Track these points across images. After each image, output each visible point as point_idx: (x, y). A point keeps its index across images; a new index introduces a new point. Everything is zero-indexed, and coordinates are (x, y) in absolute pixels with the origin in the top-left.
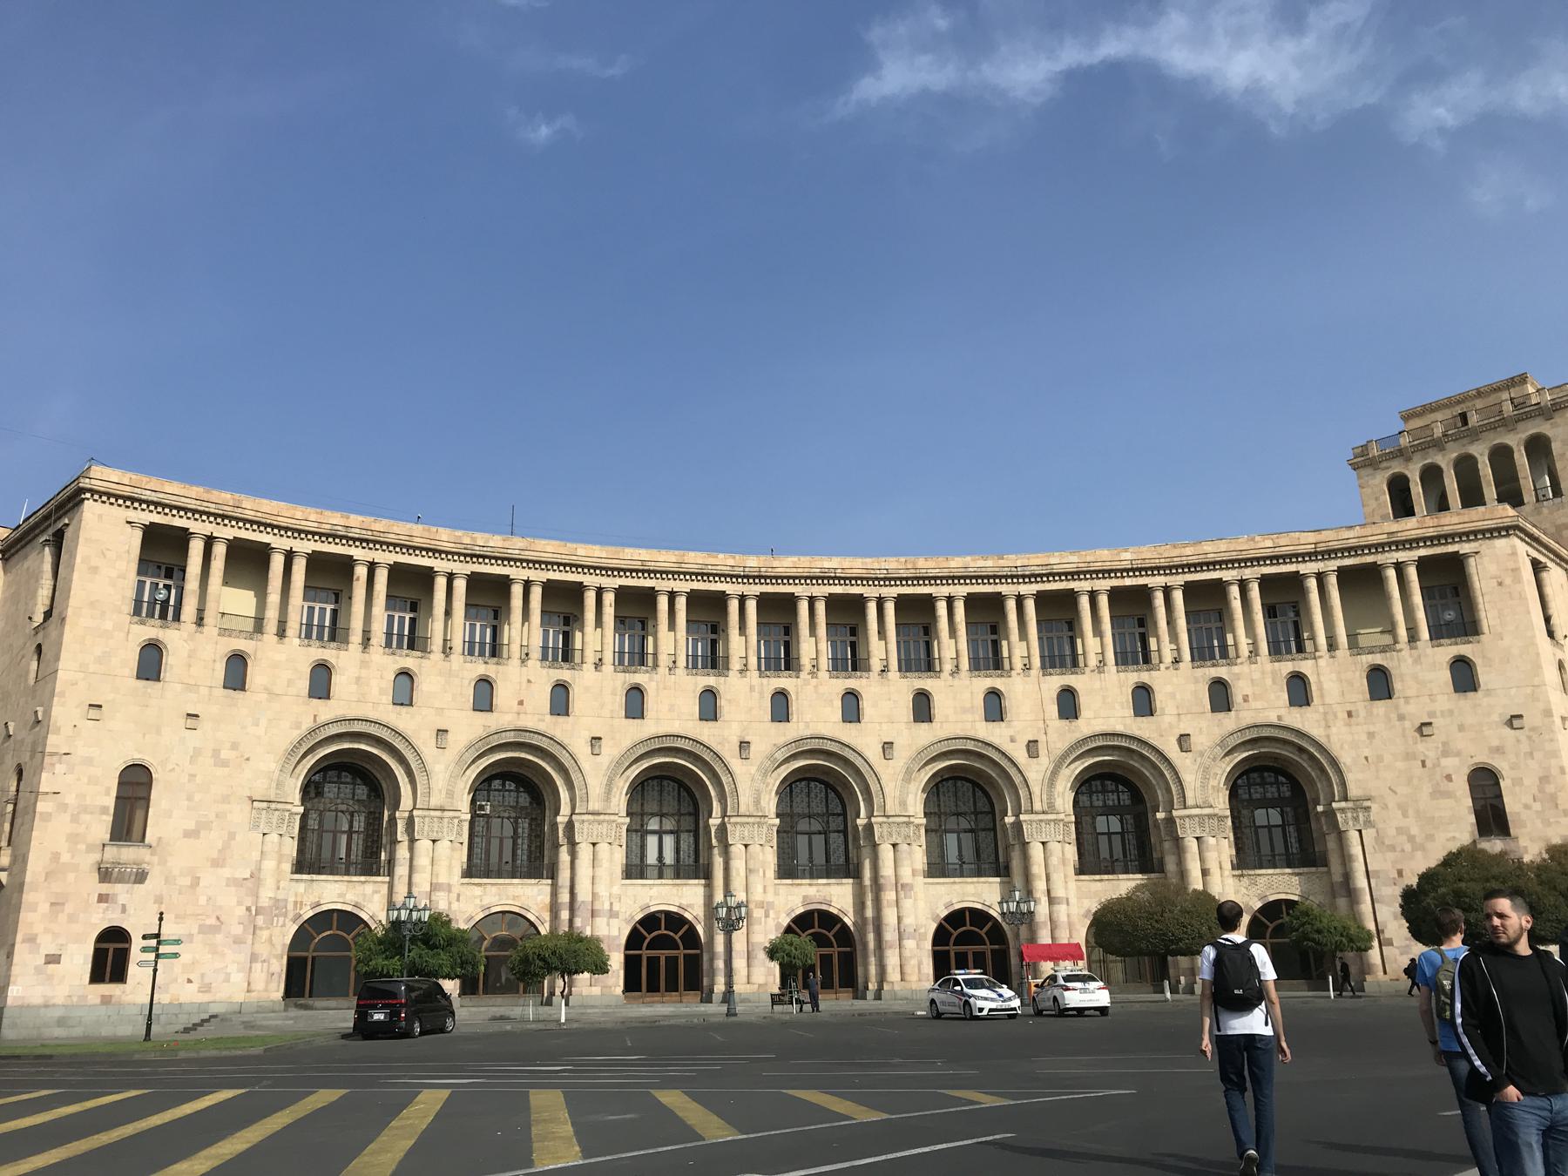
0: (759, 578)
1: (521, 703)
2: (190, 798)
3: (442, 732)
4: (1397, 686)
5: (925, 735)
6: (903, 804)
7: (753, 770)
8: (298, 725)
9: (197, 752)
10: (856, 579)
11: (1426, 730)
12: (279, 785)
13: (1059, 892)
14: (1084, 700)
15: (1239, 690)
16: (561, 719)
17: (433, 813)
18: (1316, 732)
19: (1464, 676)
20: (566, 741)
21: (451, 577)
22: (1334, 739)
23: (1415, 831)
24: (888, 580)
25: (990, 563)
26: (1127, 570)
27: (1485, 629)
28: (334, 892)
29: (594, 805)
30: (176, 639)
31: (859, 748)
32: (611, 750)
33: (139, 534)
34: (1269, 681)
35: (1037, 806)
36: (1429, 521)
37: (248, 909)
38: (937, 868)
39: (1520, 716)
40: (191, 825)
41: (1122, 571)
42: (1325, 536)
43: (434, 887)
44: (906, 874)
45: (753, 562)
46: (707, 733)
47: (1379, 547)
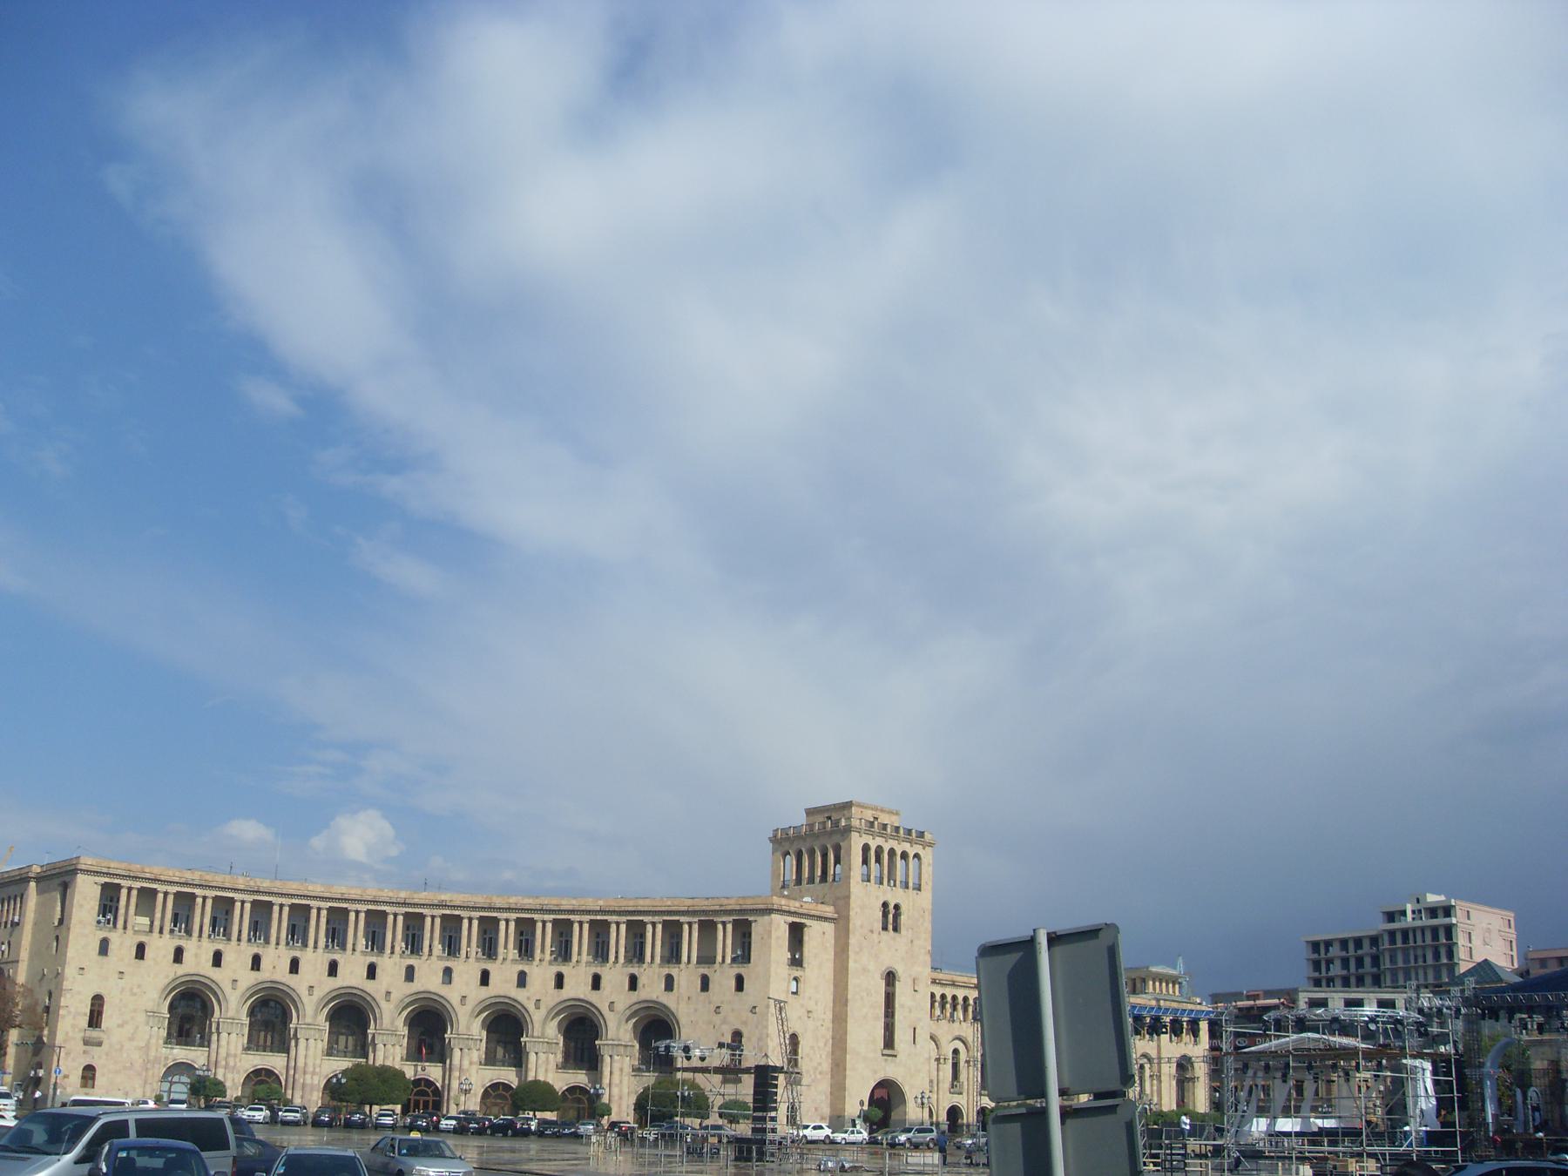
0: (405, 904)
5: (485, 993)
6: (468, 1028)
9: (123, 990)
14: (566, 980)
15: (641, 981)
18: (672, 1005)
19: (740, 983)
21: (243, 902)
24: (474, 908)
28: (181, 1053)
29: (308, 1020)
30: (115, 937)
32: (319, 993)
38: (490, 1060)
44: (466, 1063)
46: (369, 986)
47: (716, 913)
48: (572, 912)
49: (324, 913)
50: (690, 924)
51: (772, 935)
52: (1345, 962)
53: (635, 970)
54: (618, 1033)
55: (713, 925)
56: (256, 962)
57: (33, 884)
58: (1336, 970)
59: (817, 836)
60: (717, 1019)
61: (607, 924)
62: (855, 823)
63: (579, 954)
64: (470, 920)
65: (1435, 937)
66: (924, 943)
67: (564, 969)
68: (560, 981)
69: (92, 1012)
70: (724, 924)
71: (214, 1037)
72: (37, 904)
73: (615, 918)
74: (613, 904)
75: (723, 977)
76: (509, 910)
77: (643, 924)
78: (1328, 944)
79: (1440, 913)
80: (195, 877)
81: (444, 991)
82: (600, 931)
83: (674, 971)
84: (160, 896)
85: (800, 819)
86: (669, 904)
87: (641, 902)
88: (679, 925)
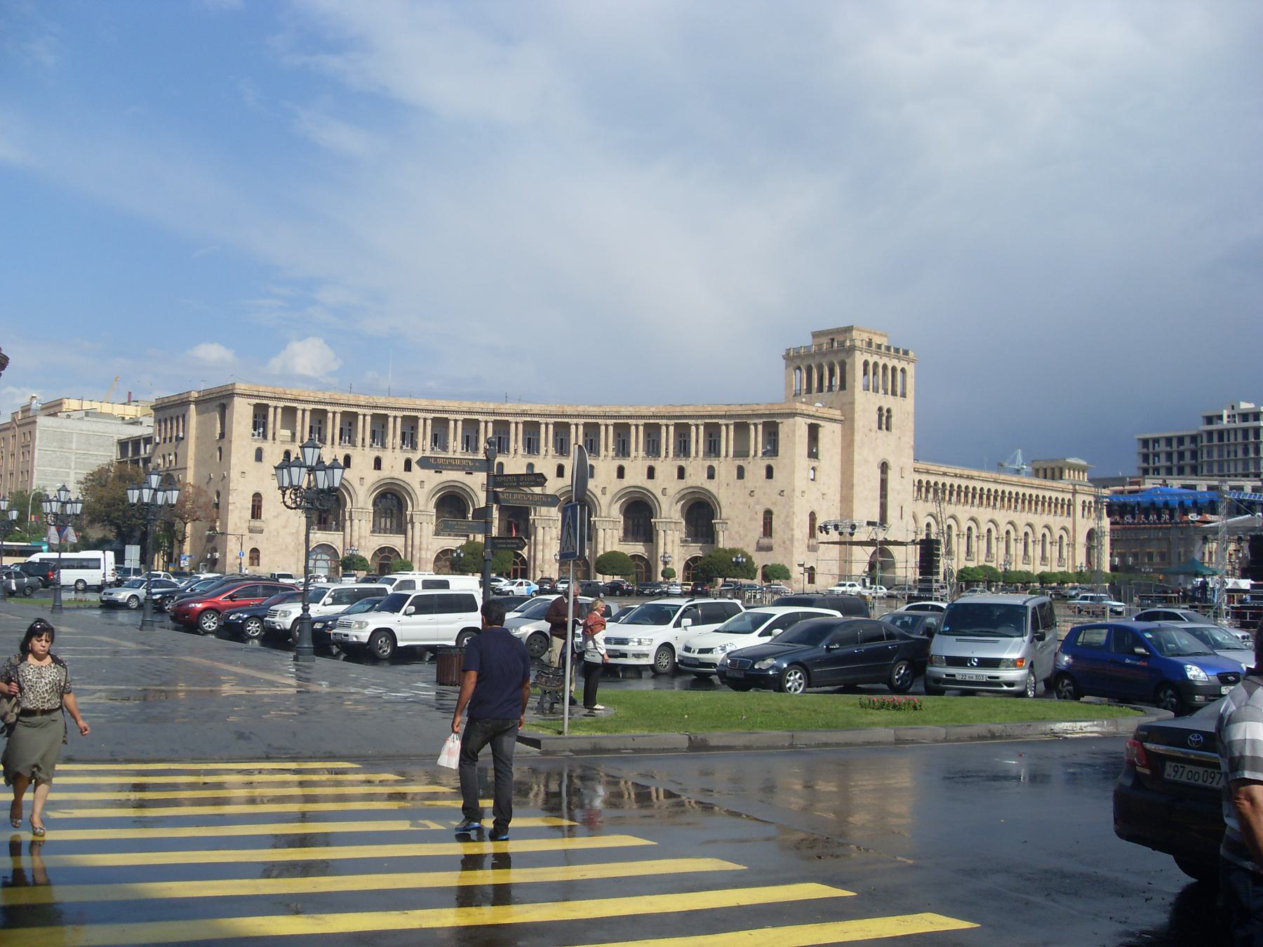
0: (494, 413)
3: (362, 479)
14: (626, 471)
18: (714, 491)
19: (770, 472)
24: (550, 416)
29: (421, 508)
30: (267, 447)
32: (429, 486)
44: (547, 539)
45: (491, 406)
47: (748, 416)
49: (429, 422)
50: (727, 426)
51: (794, 434)
52: (1169, 456)
53: (682, 463)
54: (670, 515)
55: (746, 426)
56: (378, 464)
57: (193, 407)
58: (1163, 462)
59: (824, 354)
60: (751, 501)
61: (658, 426)
62: (858, 343)
63: (637, 450)
64: (547, 425)
65: (1246, 437)
66: (909, 439)
67: (624, 463)
68: (621, 472)
70: (756, 425)
71: (348, 524)
72: (198, 423)
73: (664, 422)
74: (663, 410)
75: (756, 467)
77: (688, 426)
78: (1156, 441)
79: (1251, 418)
80: (326, 396)
82: (652, 432)
83: (715, 463)
84: (300, 413)
85: (807, 341)
86: (709, 410)
87: (686, 408)
88: (718, 426)
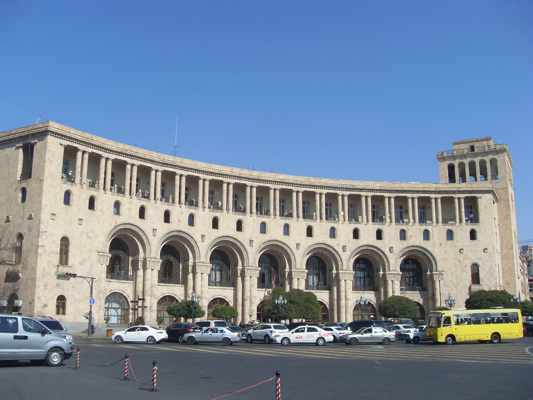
0: (258, 180)
1: (179, 221)
2: (80, 250)
4: (455, 236)
7: (254, 250)
8: (111, 225)
9: (82, 233)
10: (290, 183)
11: (461, 251)
12: (106, 246)
13: (348, 297)
15: (409, 234)
16: (192, 227)
17: (153, 260)
18: (430, 249)
19: (473, 235)
20: (193, 236)
22: (435, 251)
23: (455, 282)
24: (301, 185)
25: (334, 182)
26: (378, 190)
27: (480, 221)
28: (117, 286)
30: (75, 190)
31: (288, 245)
33: (63, 148)
34: (418, 232)
35: (344, 268)
36: (469, 186)
37: (98, 291)
39: (487, 249)
40: (81, 260)
41: (376, 190)
42: (439, 186)
43: (152, 286)
48: (361, 190)
69: (61, 250)
73: (386, 195)
76: (322, 187)
81: (285, 239)
